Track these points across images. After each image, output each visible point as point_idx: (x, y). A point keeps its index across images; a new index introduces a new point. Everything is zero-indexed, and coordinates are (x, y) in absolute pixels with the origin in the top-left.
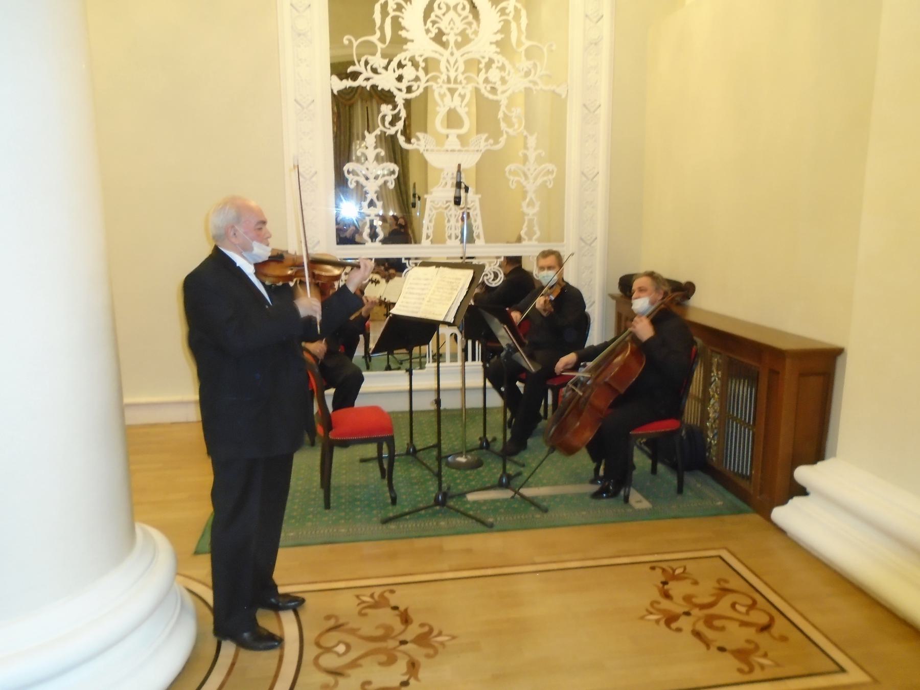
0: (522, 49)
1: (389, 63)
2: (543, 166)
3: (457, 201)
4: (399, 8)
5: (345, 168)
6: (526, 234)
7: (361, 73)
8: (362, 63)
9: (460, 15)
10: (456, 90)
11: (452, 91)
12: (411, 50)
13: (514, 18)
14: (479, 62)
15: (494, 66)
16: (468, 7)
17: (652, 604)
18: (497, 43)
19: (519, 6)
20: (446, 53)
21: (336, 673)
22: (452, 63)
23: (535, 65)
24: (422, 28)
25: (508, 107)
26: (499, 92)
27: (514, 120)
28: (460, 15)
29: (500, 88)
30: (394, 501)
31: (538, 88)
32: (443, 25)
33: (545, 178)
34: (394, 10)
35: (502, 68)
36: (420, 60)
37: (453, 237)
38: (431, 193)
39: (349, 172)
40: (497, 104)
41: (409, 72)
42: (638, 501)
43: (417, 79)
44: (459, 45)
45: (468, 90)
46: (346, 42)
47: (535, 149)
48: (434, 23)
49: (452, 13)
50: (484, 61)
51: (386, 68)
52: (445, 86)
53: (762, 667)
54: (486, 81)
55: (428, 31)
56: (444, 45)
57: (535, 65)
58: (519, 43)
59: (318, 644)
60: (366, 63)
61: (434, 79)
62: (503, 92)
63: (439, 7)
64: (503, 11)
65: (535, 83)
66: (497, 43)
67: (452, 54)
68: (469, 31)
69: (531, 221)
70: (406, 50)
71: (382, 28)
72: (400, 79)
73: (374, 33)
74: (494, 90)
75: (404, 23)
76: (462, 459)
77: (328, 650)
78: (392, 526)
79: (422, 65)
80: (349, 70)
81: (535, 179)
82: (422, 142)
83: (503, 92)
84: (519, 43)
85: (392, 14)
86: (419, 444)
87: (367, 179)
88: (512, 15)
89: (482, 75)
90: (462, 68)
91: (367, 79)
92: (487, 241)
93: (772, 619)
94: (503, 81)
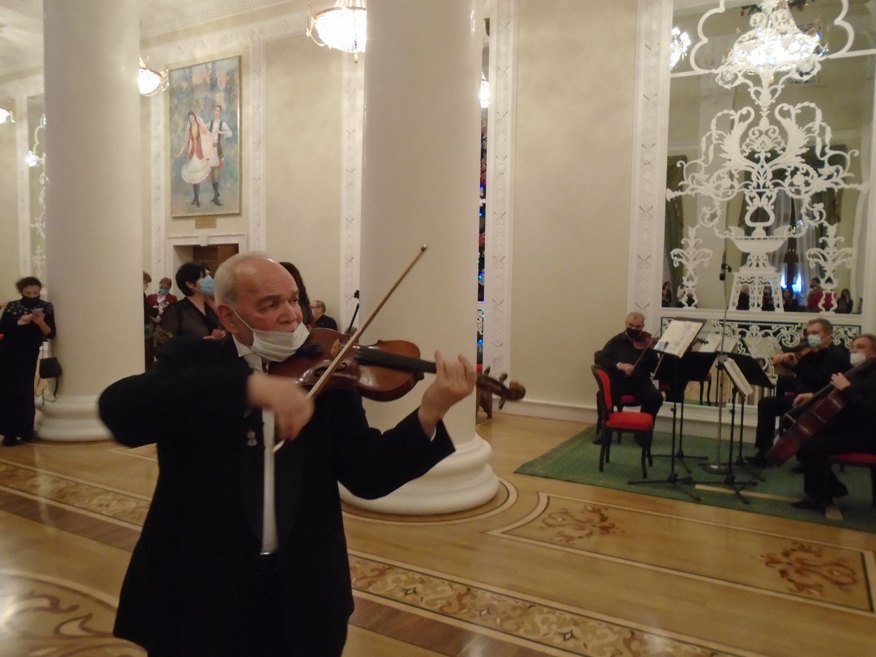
0: (825, 159)
1: (710, 177)
2: (842, 250)
3: (722, 277)
4: (721, 137)
5: (672, 253)
6: (823, 305)
7: (687, 186)
8: (690, 179)
9: (770, 138)
10: (764, 193)
11: (760, 194)
12: (729, 165)
13: (819, 135)
14: (785, 171)
15: (798, 173)
16: (777, 130)
17: (768, 556)
18: (803, 156)
19: (824, 124)
20: (757, 167)
21: (550, 525)
22: (762, 174)
23: (837, 171)
24: (738, 149)
25: (811, 204)
26: (802, 192)
27: (817, 214)
28: (770, 138)
29: (803, 189)
30: (645, 475)
31: (840, 187)
32: (756, 147)
33: (844, 260)
34: (717, 140)
35: (807, 174)
36: (735, 173)
37: (756, 305)
38: (738, 271)
39: (675, 256)
40: (800, 202)
41: (726, 182)
42: (834, 515)
43: (732, 187)
44: (768, 160)
45: (774, 192)
46: (678, 165)
47: (835, 236)
48: (748, 146)
49: (764, 137)
50: (789, 170)
51: (707, 181)
52: (755, 191)
53: (810, 593)
54: (791, 184)
55: (743, 152)
56: (757, 161)
57: (837, 171)
58: (823, 154)
59: (550, 516)
60: (693, 178)
61: (746, 186)
62: (806, 192)
63: (754, 134)
64: (809, 131)
65: (837, 184)
66: (803, 156)
67: (762, 167)
68: (778, 149)
69: (828, 296)
70: (723, 167)
71: (706, 154)
72: (718, 187)
73: (701, 157)
74: (798, 192)
75: (723, 148)
76: (715, 467)
77: (553, 518)
78: (633, 487)
79: (737, 176)
80: (680, 184)
81: (834, 260)
82: (733, 233)
83: (806, 192)
84: (823, 154)
85: (715, 142)
86: (687, 452)
87: (688, 260)
88: (817, 132)
89: (788, 180)
90: (770, 176)
91: (693, 190)
92: (785, 310)
93: (855, 582)
94: (807, 184)
